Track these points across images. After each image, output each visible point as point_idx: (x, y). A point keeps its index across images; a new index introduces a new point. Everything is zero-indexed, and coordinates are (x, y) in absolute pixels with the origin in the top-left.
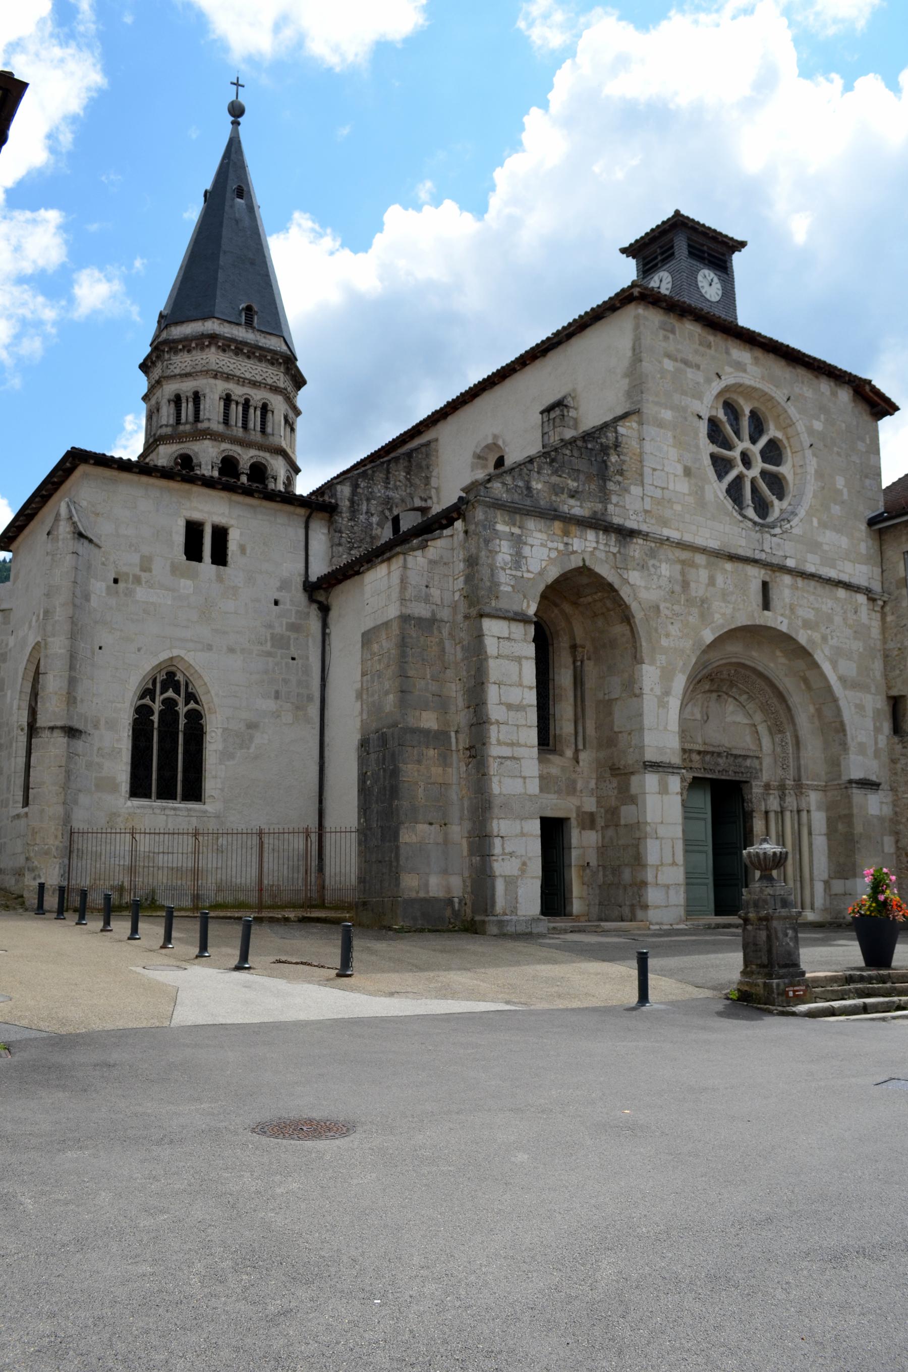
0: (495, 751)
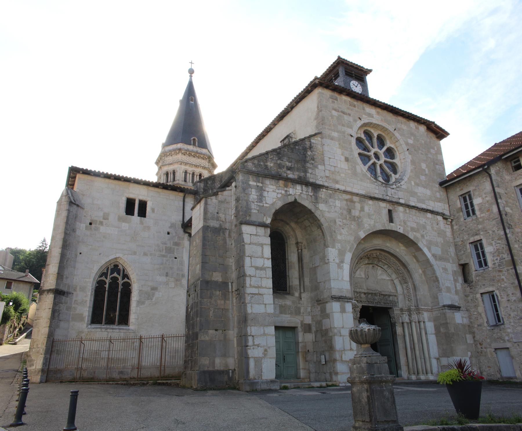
0: (249, 290)
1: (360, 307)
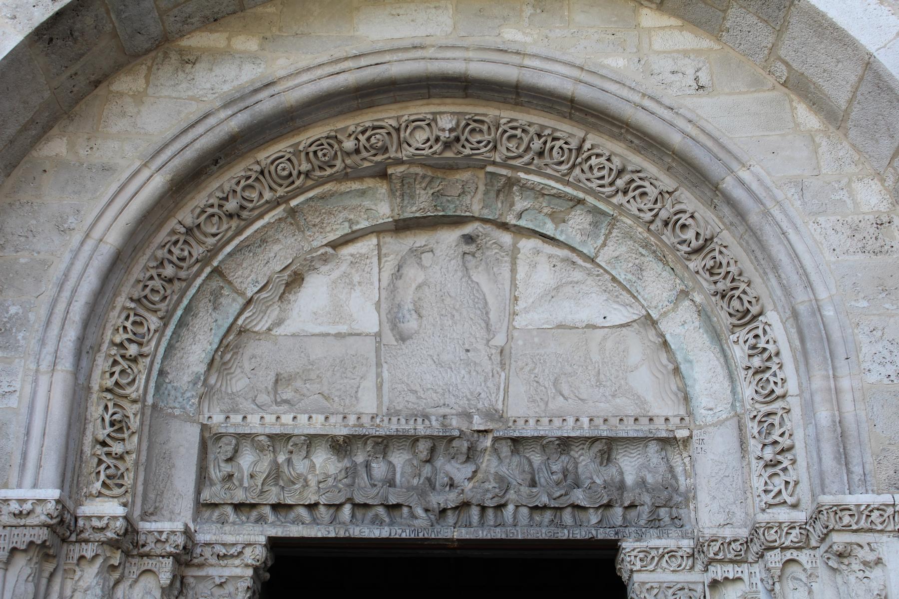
1: (257, 554)
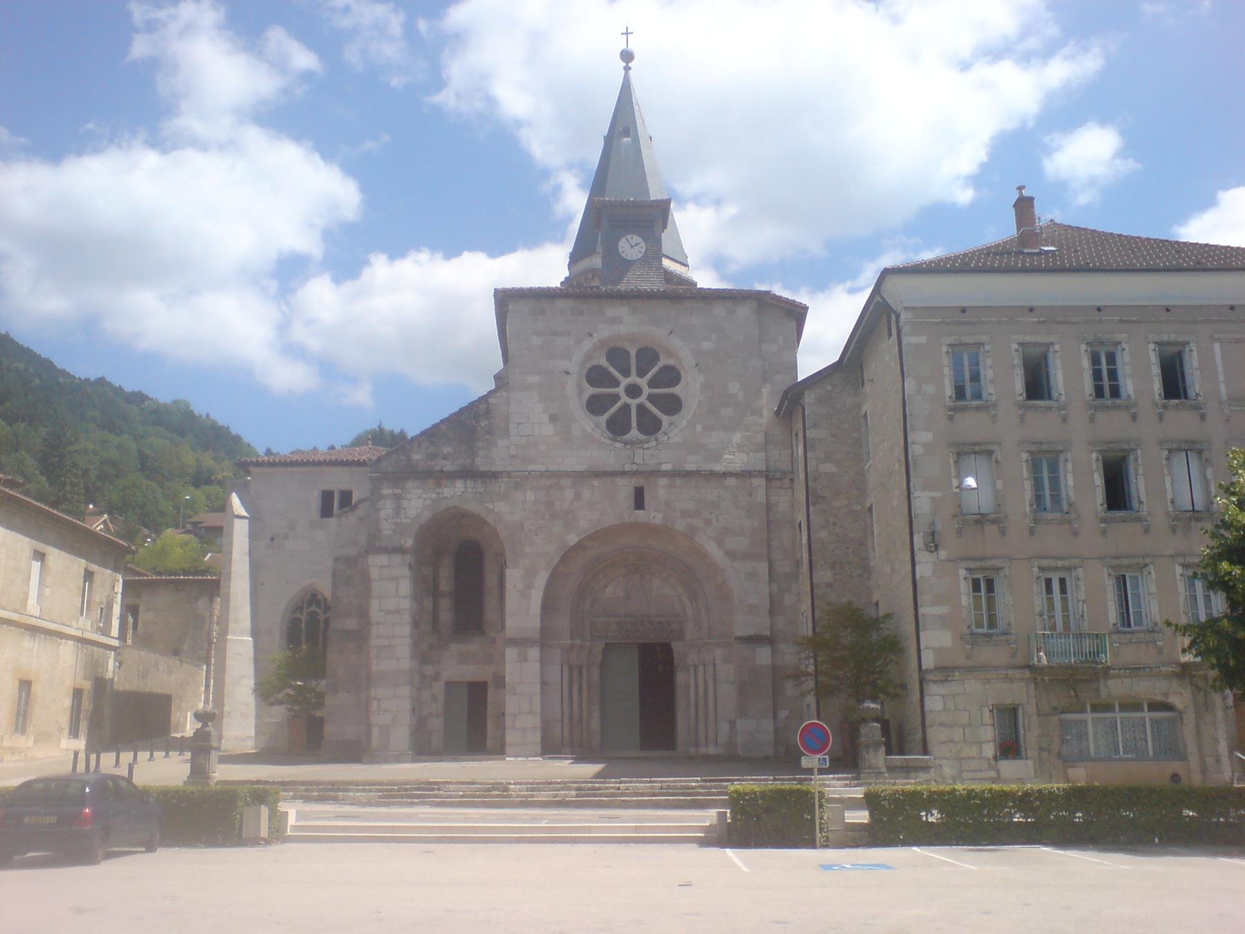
0: (374, 642)
